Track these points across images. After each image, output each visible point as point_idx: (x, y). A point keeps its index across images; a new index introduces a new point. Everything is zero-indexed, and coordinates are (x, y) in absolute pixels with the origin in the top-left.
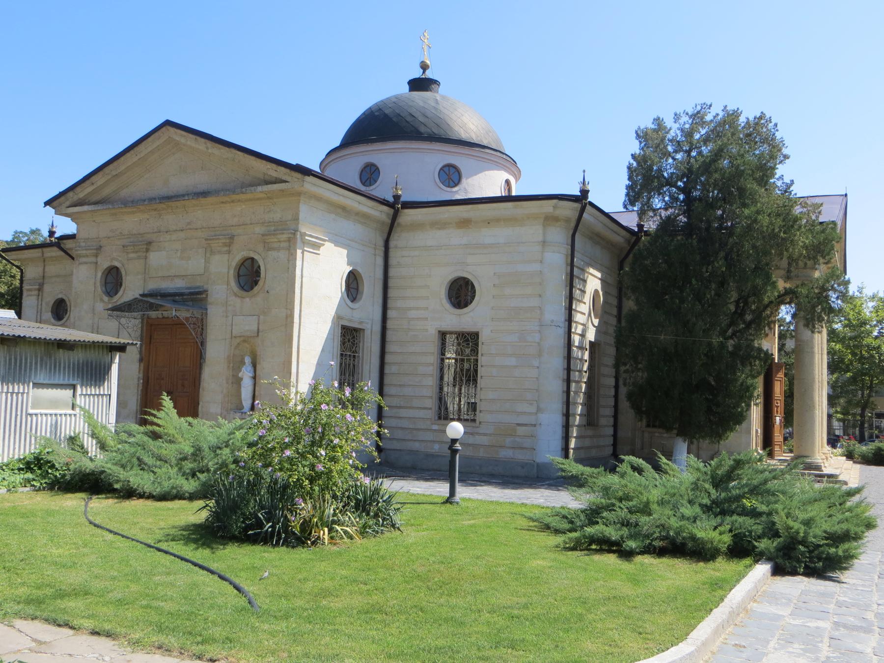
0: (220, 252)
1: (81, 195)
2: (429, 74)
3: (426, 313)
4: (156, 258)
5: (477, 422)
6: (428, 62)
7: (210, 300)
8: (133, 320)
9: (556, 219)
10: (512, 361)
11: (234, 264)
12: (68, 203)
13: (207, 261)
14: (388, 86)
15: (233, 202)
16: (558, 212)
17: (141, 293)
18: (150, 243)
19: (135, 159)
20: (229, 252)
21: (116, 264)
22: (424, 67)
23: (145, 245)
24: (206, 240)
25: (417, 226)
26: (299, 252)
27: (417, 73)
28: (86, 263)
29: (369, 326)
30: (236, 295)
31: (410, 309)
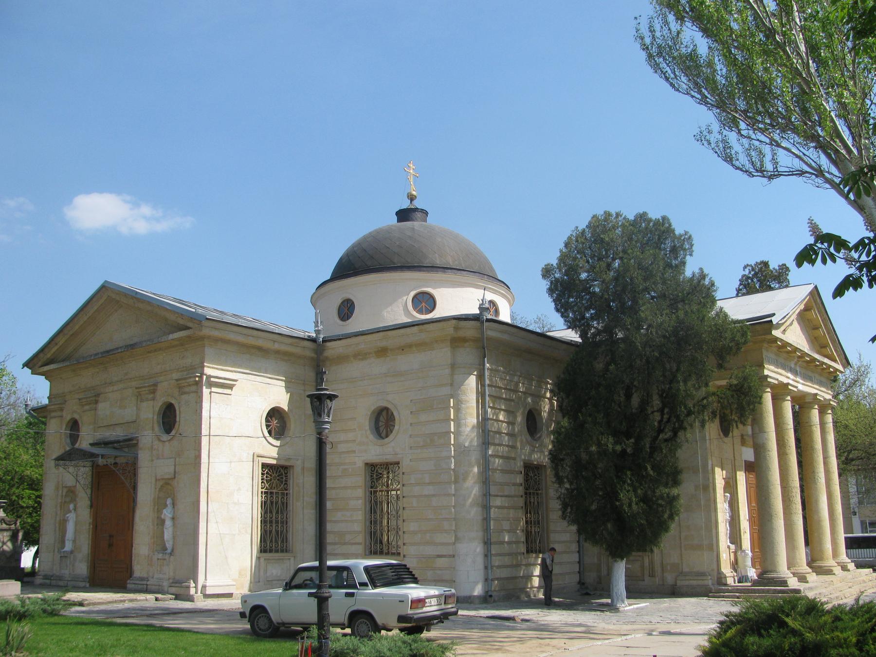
0: (147, 400)
1: (49, 356)
2: (417, 204)
3: (354, 447)
4: (104, 408)
5: (402, 555)
6: (414, 193)
7: (141, 445)
8: (82, 469)
9: (464, 340)
10: (429, 490)
11: (157, 409)
12: (40, 363)
13: (138, 409)
14: (377, 218)
15: (155, 351)
16: (461, 334)
17: (92, 442)
18: (98, 395)
19: (85, 318)
20: (153, 399)
21: (76, 416)
22: (412, 198)
23: (93, 398)
24: (137, 388)
25: (342, 359)
26: (206, 391)
27: (406, 204)
28: (55, 417)
29: (299, 463)
30: (159, 440)
31: (341, 442)
